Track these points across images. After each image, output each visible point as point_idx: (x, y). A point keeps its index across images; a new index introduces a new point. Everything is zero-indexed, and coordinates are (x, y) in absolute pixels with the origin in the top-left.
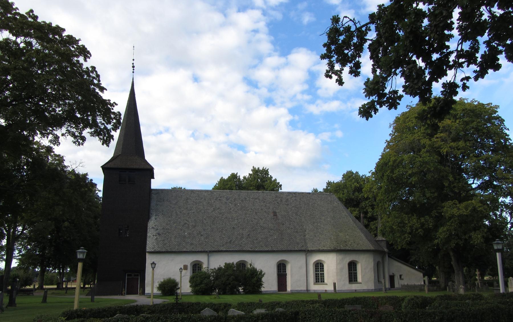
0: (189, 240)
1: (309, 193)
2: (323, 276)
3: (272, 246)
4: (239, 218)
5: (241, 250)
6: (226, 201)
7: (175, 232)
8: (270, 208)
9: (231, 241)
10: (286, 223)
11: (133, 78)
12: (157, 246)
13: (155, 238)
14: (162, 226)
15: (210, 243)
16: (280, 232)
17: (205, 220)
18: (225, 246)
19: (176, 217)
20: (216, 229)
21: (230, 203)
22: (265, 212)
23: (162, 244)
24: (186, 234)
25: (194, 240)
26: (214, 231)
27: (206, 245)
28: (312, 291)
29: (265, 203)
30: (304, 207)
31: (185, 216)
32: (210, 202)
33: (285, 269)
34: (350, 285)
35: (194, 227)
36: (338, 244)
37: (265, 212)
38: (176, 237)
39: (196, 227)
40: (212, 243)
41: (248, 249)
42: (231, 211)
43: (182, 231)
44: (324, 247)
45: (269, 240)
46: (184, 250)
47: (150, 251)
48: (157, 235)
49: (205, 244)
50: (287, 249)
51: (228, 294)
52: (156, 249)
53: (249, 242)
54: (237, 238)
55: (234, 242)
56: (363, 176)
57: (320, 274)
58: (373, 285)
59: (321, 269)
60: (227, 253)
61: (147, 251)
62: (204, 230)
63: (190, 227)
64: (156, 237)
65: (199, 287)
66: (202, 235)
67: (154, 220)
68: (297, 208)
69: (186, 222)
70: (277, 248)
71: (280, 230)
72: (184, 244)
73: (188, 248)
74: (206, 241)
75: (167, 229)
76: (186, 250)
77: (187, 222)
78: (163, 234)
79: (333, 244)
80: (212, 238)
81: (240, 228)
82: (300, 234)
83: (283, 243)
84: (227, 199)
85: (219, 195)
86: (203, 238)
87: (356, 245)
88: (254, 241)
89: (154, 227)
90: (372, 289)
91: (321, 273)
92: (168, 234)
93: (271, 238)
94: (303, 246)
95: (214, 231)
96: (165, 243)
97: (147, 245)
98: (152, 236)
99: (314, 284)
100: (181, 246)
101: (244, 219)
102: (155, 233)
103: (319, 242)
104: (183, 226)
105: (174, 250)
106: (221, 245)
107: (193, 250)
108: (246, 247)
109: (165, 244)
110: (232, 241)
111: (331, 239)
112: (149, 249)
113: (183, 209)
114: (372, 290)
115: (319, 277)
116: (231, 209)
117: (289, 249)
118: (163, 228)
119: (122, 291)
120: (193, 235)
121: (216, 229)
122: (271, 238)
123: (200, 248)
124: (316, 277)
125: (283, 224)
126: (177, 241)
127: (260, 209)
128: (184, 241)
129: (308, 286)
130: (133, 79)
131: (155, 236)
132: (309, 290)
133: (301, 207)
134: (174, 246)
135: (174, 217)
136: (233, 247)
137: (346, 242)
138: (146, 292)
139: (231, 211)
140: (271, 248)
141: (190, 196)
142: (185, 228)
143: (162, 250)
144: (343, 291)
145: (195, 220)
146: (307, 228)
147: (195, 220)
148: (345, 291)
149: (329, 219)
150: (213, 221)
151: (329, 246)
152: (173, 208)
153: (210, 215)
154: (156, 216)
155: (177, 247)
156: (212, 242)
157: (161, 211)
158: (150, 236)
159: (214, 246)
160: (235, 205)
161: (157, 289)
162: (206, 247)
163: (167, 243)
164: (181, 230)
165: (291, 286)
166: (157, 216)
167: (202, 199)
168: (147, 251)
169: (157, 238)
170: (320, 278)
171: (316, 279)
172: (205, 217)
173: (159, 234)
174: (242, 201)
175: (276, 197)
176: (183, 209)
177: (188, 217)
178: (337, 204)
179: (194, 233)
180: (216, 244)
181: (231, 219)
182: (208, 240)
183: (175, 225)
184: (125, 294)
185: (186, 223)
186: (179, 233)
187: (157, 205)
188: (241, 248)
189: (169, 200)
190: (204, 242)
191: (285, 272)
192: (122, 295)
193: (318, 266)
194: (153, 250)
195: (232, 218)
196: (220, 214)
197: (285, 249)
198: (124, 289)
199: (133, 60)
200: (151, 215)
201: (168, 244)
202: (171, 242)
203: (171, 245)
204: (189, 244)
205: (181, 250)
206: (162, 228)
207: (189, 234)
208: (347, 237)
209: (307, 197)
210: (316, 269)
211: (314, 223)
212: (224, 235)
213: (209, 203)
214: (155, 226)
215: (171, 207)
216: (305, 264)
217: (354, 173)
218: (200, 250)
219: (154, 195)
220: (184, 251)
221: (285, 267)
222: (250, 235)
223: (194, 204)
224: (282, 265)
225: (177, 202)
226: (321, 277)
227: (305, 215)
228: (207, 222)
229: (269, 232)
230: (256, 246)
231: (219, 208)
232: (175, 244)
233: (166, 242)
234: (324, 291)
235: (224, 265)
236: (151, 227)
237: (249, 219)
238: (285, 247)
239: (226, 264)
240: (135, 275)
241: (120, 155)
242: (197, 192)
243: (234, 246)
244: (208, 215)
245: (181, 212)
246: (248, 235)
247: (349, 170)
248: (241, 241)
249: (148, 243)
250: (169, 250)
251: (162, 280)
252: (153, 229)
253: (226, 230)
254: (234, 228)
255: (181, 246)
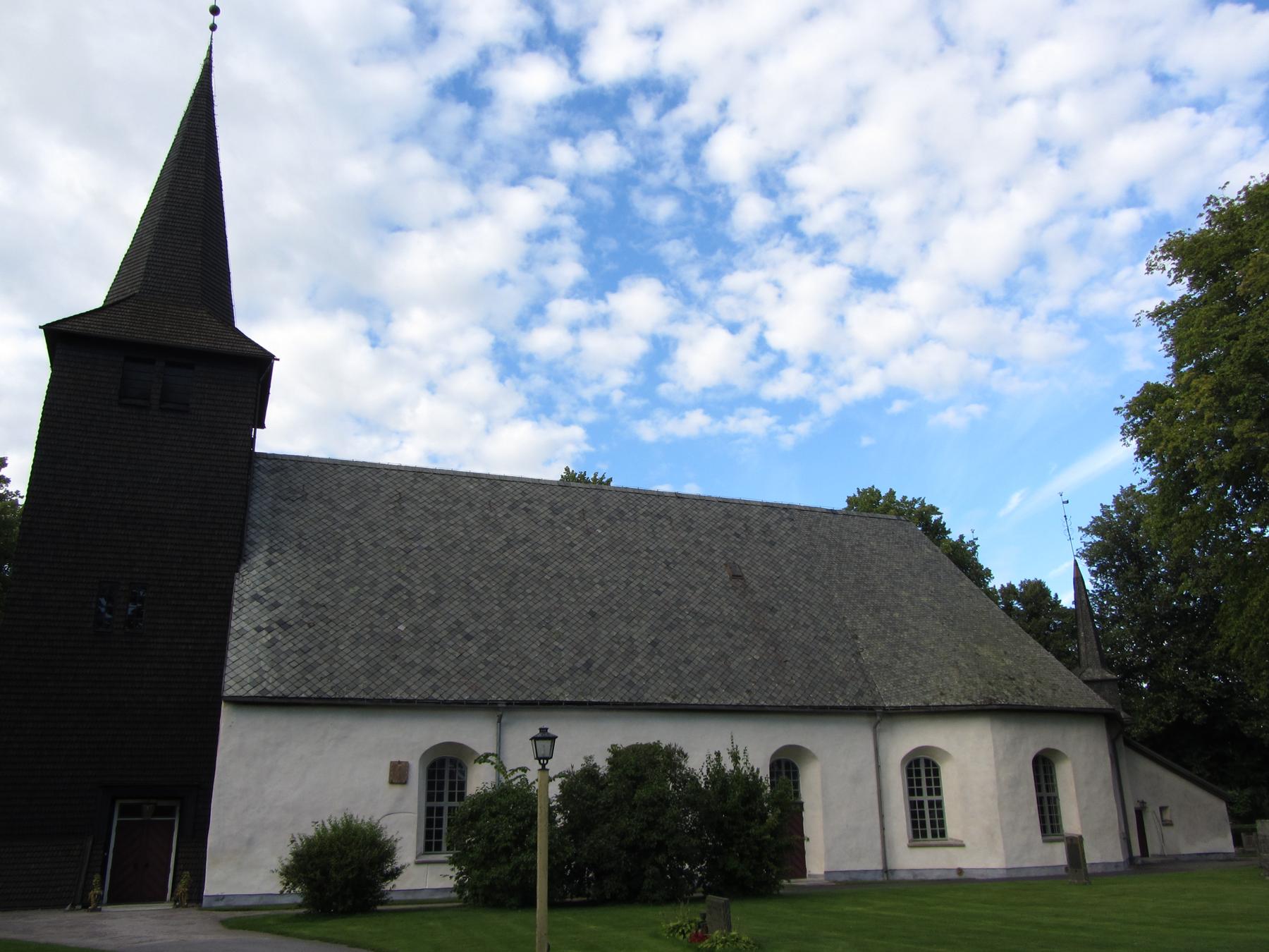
0: (417, 653)
1: (833, 512)
2: (941, 814)
3: (749, 688)
4: (608, 578)
5: (635, 700)
6: (551, 517)
7: (352, 618)
8: (714, 551)
9: (588, 664)
10: (780, 606)
11: (211, 47)
12: (276, 676)
13: (264, 640)
14: (298, 592)
15: (506, 670)
16: (767, 636)
17: (478, 577)
18: (569, 683)
19: (358, 562)
20: (525, 616)
21: (570, 524)
22: (700, 562)
23: (299, 668)
24: (402, 628)
25: (437, 654)
26: (517, 622)
27: (488, 677)
28: (909, 877)
29: (692, 534)
30: (830, 556)
31: (394, 558)
32: (492, 514)
33: (796, 785)
34: (1048, 847)
35: (437, 601)
36: (990, 683)
37: (700, 562)
38: (357, 639)
39: (442, 605)
40: (515, 670)
41: (661, 699)
42: (573, 550)
43: (386, 617)
44: (942, 694)
45: (735, 663)
46: (398, 694)
47: (241, 693)
48: (275, 626)
49: (483, 673)
50: (809, 703)
51: (656, 903)
52: (269, 688)
53: (662, 672)
54: (611, 652)
55: (602, 669)
56: (915, 501)
57: (926, 805)
58: (1119, 845)
59: (929, 782)
60: (576, 713)
61: (228, 693)
62: (477, 616)
63: (419, 601)
64: (269, 637)
65: (508, 868)
66: (468, 637)
67: (266, 566)
68: (805, 556)
69: (400, 581)
70: (771, 698)
71: (766, 631)
72: (393, 671)
73: (414, 687)
74: (490, 659)
75: (317, 606)
76: (405, 696)
77: (404, 584)
78: (300, 623)
79: (975, 685)
80: (512, 649)
81: (617, 614)
82: (840, 648)
83: (788, 678)
84: (555, 512)
85: (524, 493)
86: (475, 648)
87: (1050, 691)
88: (681, 668)
89: (262, 593)
90: (1114, 861)
91: (931, 798)
92: (322, 624)
93: (739, 660)
94: (861, 693)
95: (517, 622)
96: (310, 661)
97: (227, 670)
98: (254, 632)
99: (910, 846)
100: (383, 679)
101: (628, 583)
102: (266, 618)
103: (917, 677)
104: (388, 596)
105: (352, 694)
106: (554, 679)
107: (435, 696)
108: (653, 687)
109: (310, 668)
110: (596, 665)
111: (958, 667)
112: (237, 687)
113: (384, 534)
114: (1117, 865)
115: (922, 814)
116: (572, 545)
117: (816, 703)
118: (303, 603)
119: (87, 888)
120: (431, 635)
121: (525, 616)
122: (739, 660)
123: (465, 688)
124: (913, 815)
125: (773, 610)
126: (362, 655)
127: (678, 553)
128: (397, 657)
129: (887, 850)
130: (211, 42)
131: (264, 633)
132: (893, 871)
133: (819, 555)
134: (352, 678)
135: (348, 562)
136: (602, 690)
137: (1014, 679)
138: (210, 889)
139: (573, 550)
140: (747, 696)
141: (412, 490)
142: (396, 603)
143: (297, 693)
144: (1023, 874)
145: (436, 577)
146: (860, 627)
147: (436, 577)
148: (1033, 874)
149: (924, 599)
150: (510, 584)
151: (963, 692)
152: (343, 527)
153: (495, 562)
154: (271, 550)
155: (363, 682)
156: (514, 664)
157: (292, 533)
158: (242, 633)
159: (522, 682)
160: (588, 532)
161: (284, 879)
162: (489, 685)
163: (321, 661)
164: (381, 612)
165: (828, 851)
166: (276, 554)
167: (457, 501)
168: (228, 693)
169: (274, 638)
170: (928, 819)
171: (914, 824)
172: (474, 569)
173: (283, 624)
174: (610, 519)
175: (728, 516)
176: (384, 534)
177: (408, 562)
178: (929, 551)
179: (434, 625)
180: (530, 674)
181: (577, 582)
182: (495, 655)
183: (351, 591)
184: (100, 897)
185: (399, 588)
186: (371, 626)
187: (276, 511)
188: (632, 691)
189: (326, 498)
190: (481, 666)
191: (797, 794)
192: (85, 906)
193: (918, 773)
194: (253, 693)
195: (582, 579)
196: (535, 559)
197: (801, 703)
198: (97, 878)
199: (213, 28)
200: (251, 549)
201: (326, 665)
202: (336, 658)
203: (336, 674)
204: (418, 668)
205: (384, 696)
206: (298, 599)
207: (416, 629)
208: (1008, 662)
209: (830, 522)
210: (910, 783)
211: (877, 609)
212: (560, 638)
213: (486, 518)
214: (267, 590)
215: (335, 521)
216: (873, 766)
217: (883, 494)
218: (466, 698)
219: (263, 476)
220: (395, 700)
221: (795, 775)
222: (661, 644)
223: (431, 518)
224: (783, 766)
225: (358, 508)
226: (931, 813)
227: (841, 580)
228: (486, 588)
229: (730, 636)
230: (691, 686)
231: (526, 540)
232: (357, 666)
233: (316, 657)
234: (954, 875)
235: (610, 755)
236: (246, 596)
237: (644, 583)
238: (799, 695)
239: (615, 751)
240: (159, 811)
241: (134, 295)
242: (440, 478)
243: (604, 683)
244: (486, 561)
245: (375, 545)
246: (654, 644)
247: (865, 485)
248: (631, 667)
249: (234, 658)
250: (331, 694)
251: (311, 833)
252: (256, 603)
253: (565, 621)
254: (592, 614)
255: (383, 679)
